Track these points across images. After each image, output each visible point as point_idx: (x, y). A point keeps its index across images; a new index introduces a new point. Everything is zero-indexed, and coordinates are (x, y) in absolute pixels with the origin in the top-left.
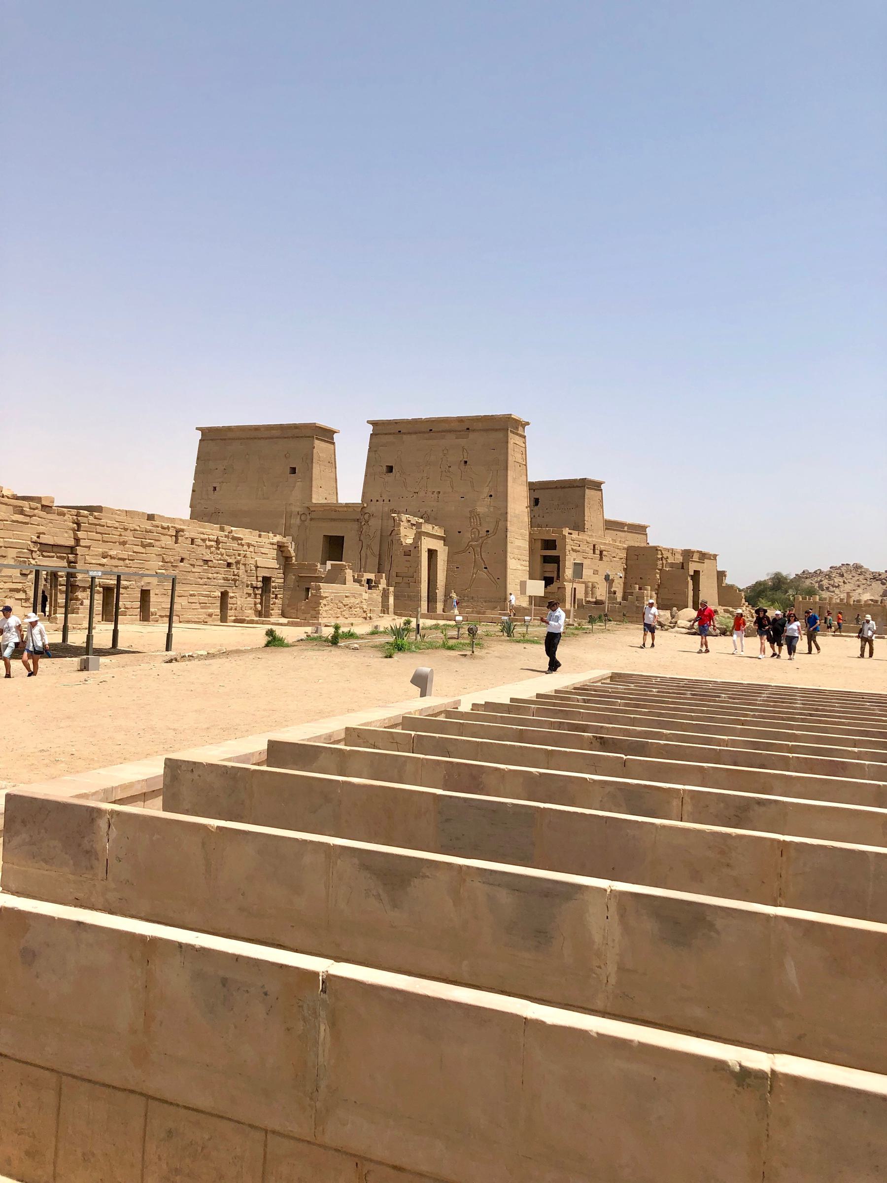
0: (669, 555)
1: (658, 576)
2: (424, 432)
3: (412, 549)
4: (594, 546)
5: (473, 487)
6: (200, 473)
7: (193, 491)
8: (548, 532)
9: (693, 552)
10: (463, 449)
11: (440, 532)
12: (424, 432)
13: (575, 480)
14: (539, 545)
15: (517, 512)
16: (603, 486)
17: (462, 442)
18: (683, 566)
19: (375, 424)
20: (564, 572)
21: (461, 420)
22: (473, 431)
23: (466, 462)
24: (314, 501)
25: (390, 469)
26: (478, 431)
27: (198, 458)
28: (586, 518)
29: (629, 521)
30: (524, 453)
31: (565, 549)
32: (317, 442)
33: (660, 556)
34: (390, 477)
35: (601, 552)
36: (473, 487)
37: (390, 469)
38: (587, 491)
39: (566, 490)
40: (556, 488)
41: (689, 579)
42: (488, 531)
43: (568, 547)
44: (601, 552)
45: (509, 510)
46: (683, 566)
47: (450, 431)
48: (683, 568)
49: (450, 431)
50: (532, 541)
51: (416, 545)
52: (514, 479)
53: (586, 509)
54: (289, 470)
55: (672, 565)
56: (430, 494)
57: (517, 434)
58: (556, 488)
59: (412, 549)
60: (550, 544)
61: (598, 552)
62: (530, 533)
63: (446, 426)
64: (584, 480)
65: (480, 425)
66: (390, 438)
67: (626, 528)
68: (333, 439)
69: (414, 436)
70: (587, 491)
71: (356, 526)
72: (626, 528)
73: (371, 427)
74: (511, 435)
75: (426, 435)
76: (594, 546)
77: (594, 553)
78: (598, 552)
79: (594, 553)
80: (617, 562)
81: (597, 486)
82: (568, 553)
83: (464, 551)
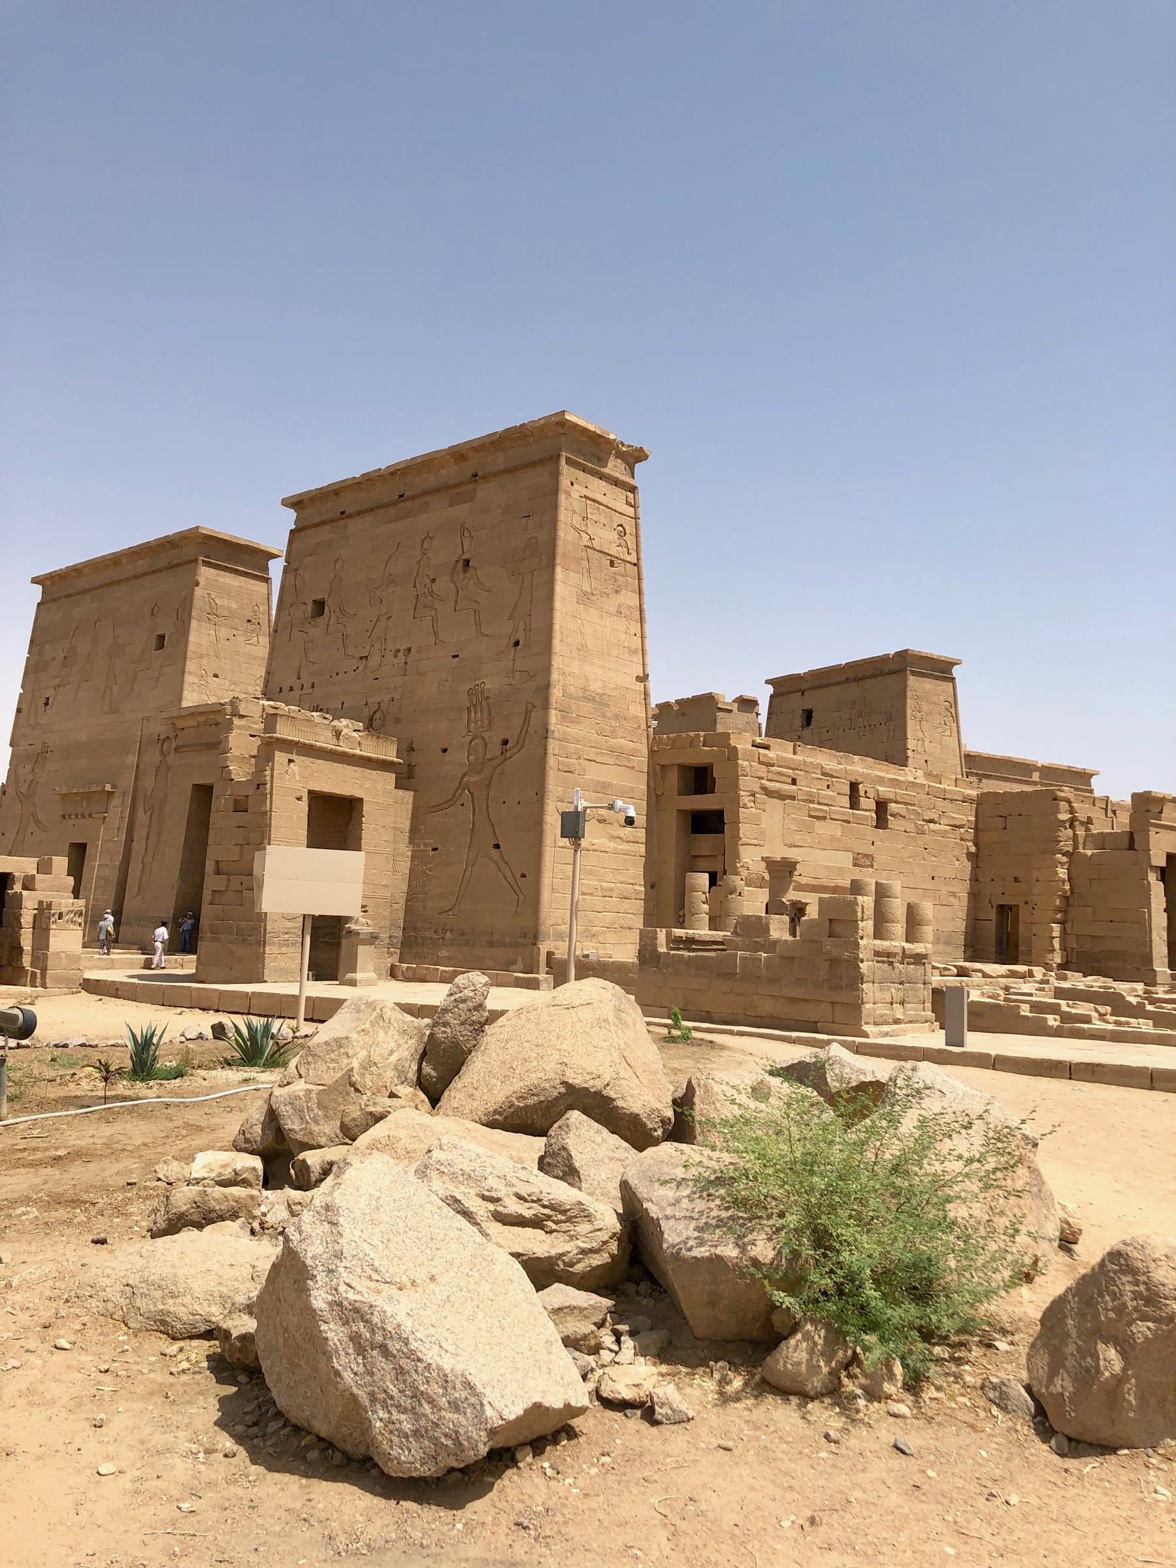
0: (1097, 814)
1: (1062, 873)
2: (387, 505)
3: (251, 791)
4: (854, 786)
5: (478, 624)
6: (34, 669)
7: (19, 711)
8: (693, 742)
9: (1161, 801)
10: (463, 529)
11: (389, 752)
12: (387, 505)
13: (884, 659)
14: (673, 779)
15: (595, 687)
16: (956, 671)
17: (462, 510)
18: (1133, 841)
19: (296, 503)
20: (737, 856)
21: (458, 454)
22: (485, 478)
23: (467, 563)
24: (185, 704)
25: (320, 607)
26: (496, 475)
27: (32, 642)
28: (911, 744)
29: (1041, 762)
30: (630, 532)
31: (736, 788)
32: (205, 574)
33: (1064, 816)
34: (316, 631)
35: (881, 806)
36: (478, 624)
37: (320, 607)
38: (912, 681)
39: (867, 683)
40: (847, 681)
41: (1152, 877)
42: (505, 742)
43: (746, 784)
44: (881, 806)
45: (555, 676)
46: (1133, 841)
47: (435, 491)
48: (1131, 846)
49: (435, 491)
50: (657, 770)
51: (259, 784)
52: (585, 598)
53: (911, 725)
54: (154, 642)
55: (1101, 841)
56: (389, 656)
57: (602, 476)
58: (847, 681)
59: (251, 791)
60: (700, 779)
61: (868, 803)
62: (651, 752)
63: (429, 480)
64: (903, 655)
65: (499, 461)
66: (326, 533)
67: (1036, 776)
68: (266, 570)
69: (368, 519)
70: (912, 681)
71: (280, 757)
72: (1036, 776)
73: (292, 515)
74: (567, 473)
75: (392, 511)
76: (854, 786)
77: (854, 804)
78: (868, 803)
79: (854, 804)
80: (944, 834)
81: (941, 670)
82: (745, 798)
83: (450, 802)
